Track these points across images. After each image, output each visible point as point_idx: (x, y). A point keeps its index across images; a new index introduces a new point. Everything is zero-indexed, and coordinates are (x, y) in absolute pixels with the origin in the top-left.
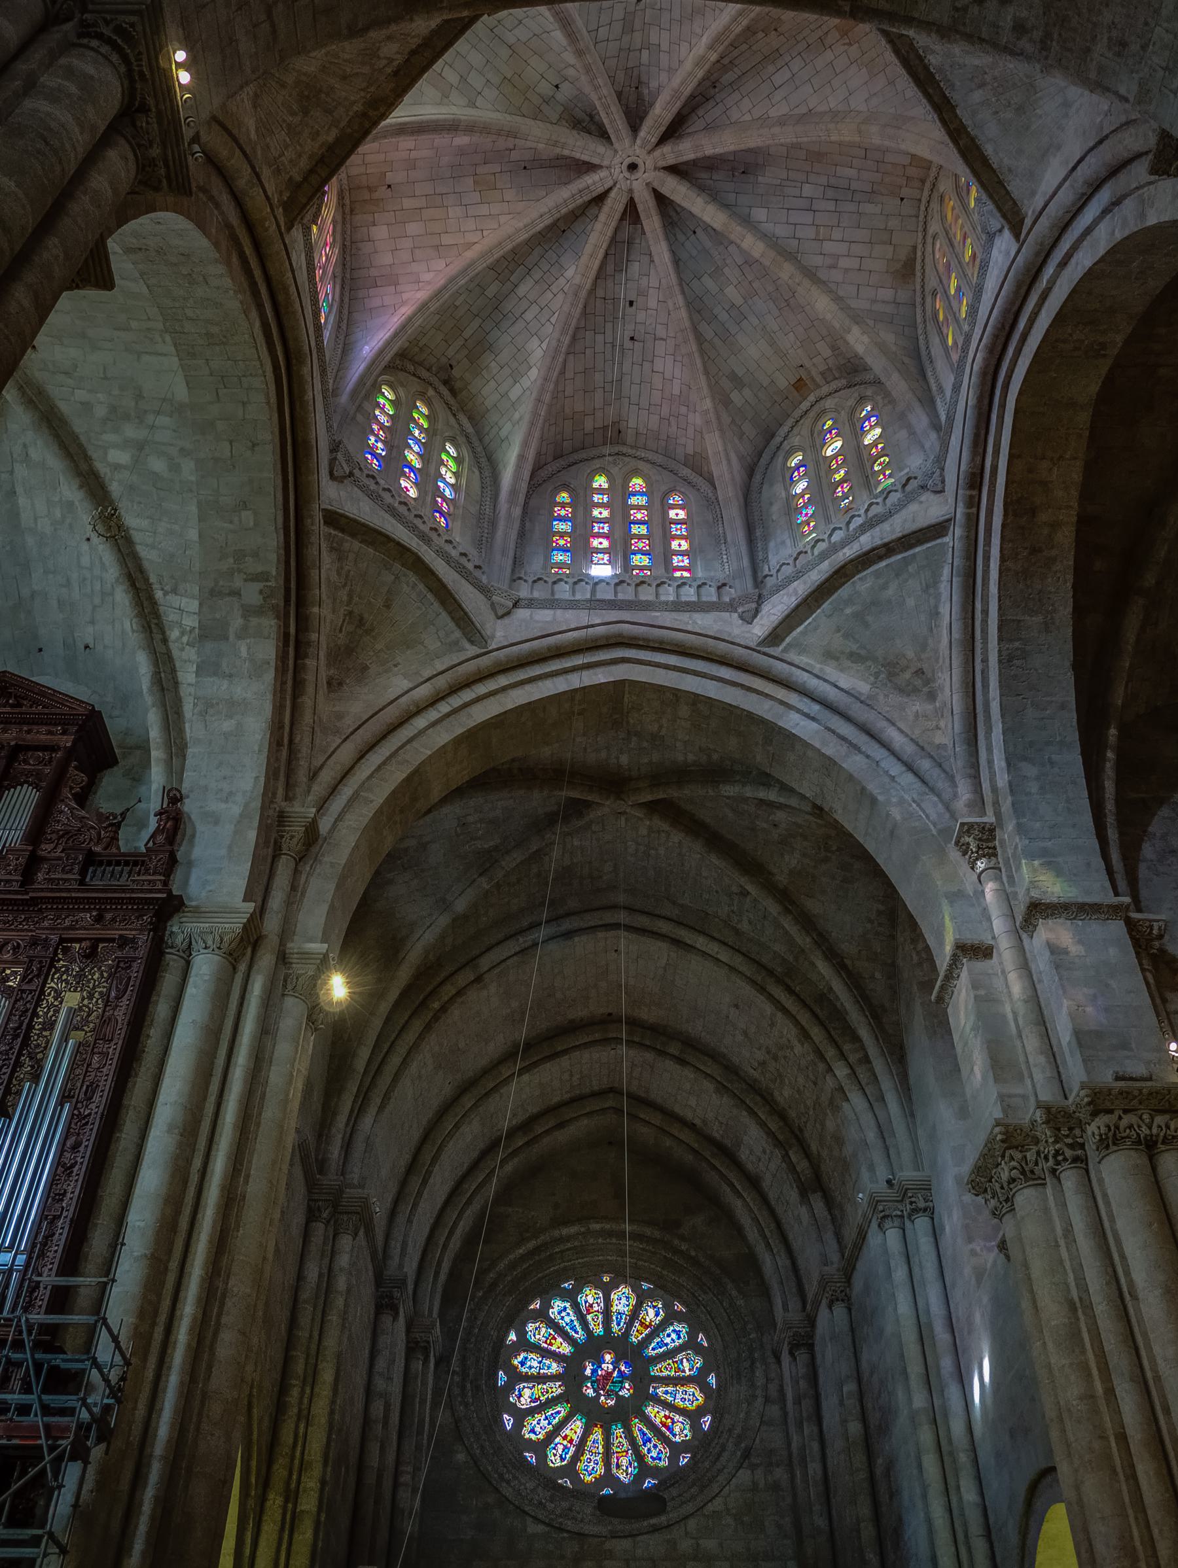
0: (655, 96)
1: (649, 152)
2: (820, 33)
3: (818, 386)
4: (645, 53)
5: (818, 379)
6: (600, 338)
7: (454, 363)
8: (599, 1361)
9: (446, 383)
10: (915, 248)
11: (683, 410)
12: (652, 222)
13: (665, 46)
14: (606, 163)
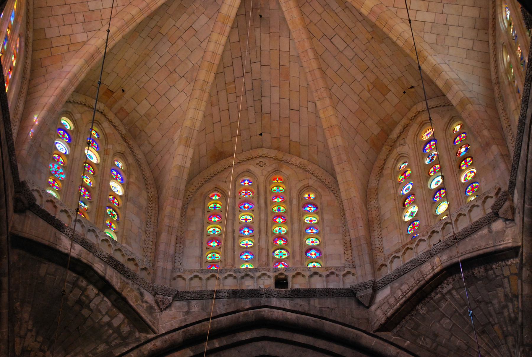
2: (372, 66)
3: (110, 108)
11: (80, 18)
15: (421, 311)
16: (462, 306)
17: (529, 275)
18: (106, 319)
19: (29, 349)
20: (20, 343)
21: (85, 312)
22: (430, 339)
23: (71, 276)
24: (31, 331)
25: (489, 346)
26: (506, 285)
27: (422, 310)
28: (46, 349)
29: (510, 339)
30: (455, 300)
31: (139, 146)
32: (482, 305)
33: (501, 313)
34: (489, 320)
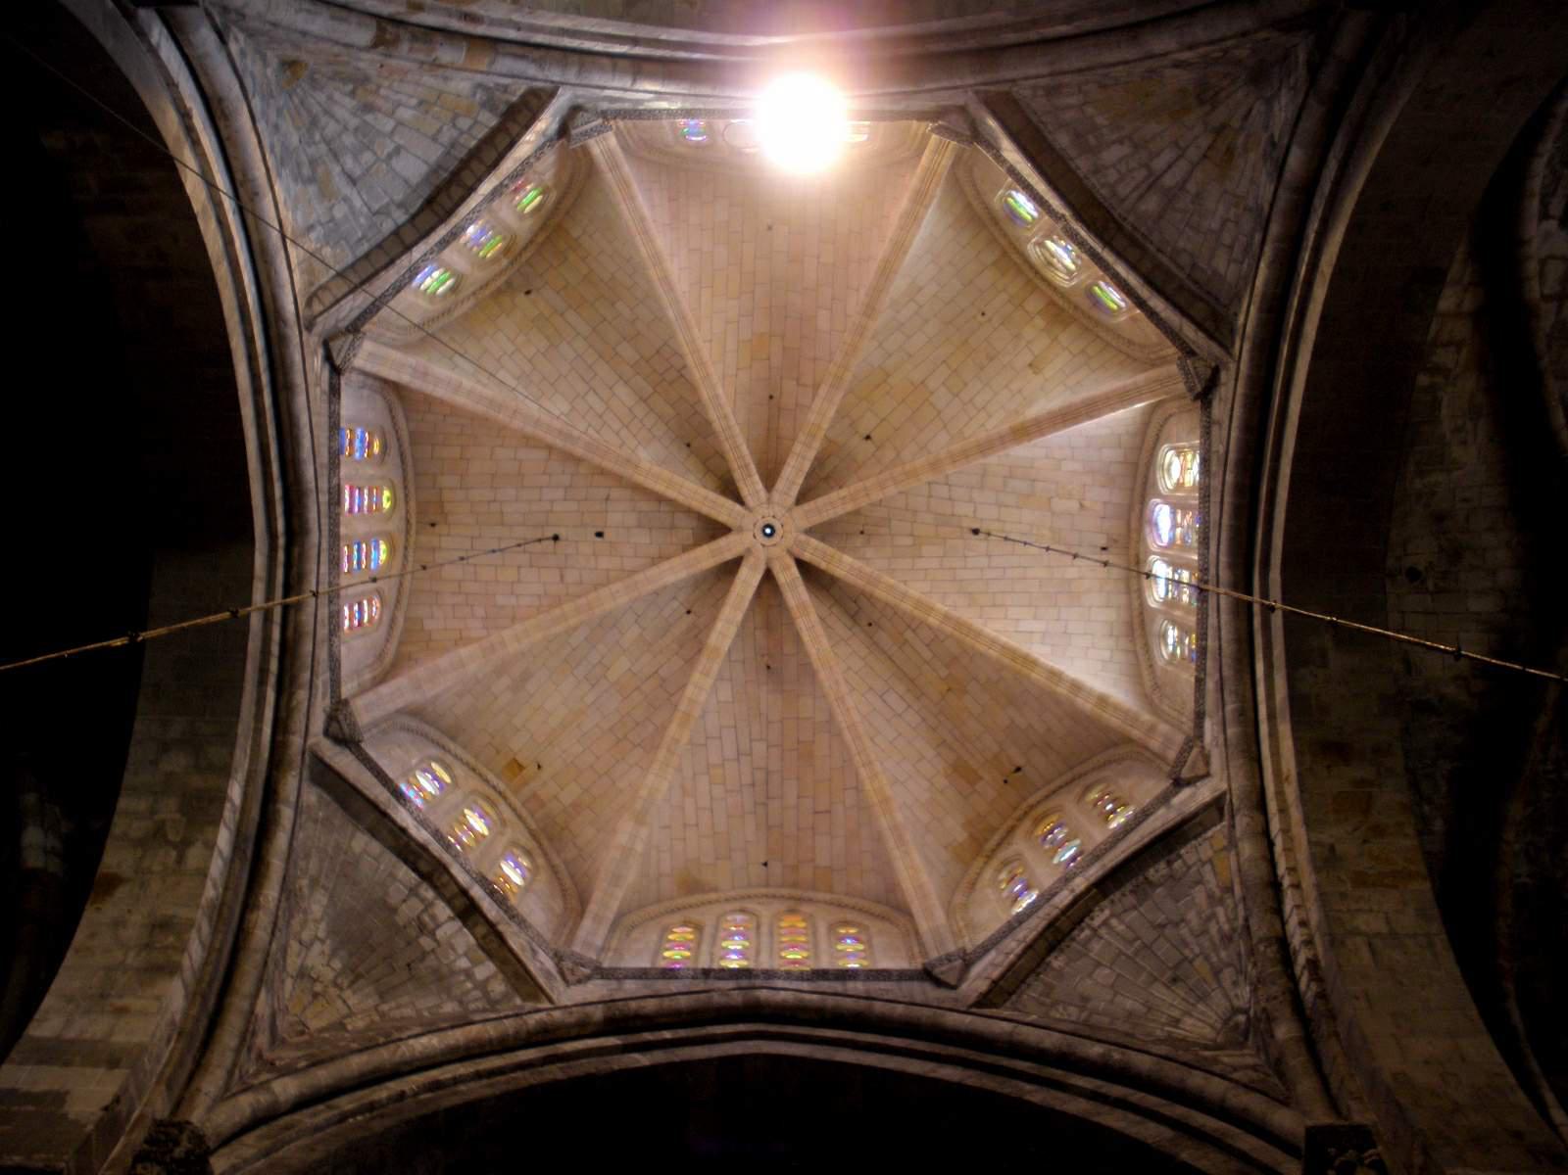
0: (854, 552)
1: (790, 552)
3: (516, 792)
4: (908, 541)
5: (526, 792)
6: (560, 494)
7: (532, 296)
9: (509, 283)
10: (715, 890)
11: (480, 612)
12: (708, 556)
13: (921, 563)
14: (776, 496)
15: (1056, 964)
16: (1131, 942)
17: (1248, 825)
18: (463, 963)
19: (315, 976)
20: (299, 955)
21: (426, 942)
22: (1076, 1006)
23: (405, 873)
24: (323, 941)
25: (1188, 1002)
26: (1209, 876)
27: (1057, 962)
28: (345, 984)
29: (1228, 975)
30: (1118, 934)
31: (558, 852)
32: (1168, 931)
33: (1205, 932)
34: (1182, 953)
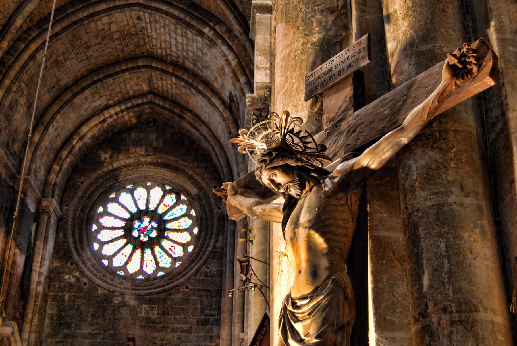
8: (141, 221)
